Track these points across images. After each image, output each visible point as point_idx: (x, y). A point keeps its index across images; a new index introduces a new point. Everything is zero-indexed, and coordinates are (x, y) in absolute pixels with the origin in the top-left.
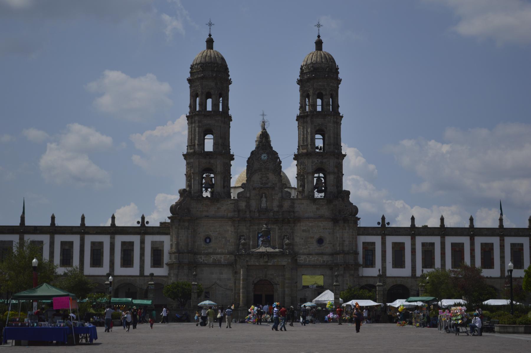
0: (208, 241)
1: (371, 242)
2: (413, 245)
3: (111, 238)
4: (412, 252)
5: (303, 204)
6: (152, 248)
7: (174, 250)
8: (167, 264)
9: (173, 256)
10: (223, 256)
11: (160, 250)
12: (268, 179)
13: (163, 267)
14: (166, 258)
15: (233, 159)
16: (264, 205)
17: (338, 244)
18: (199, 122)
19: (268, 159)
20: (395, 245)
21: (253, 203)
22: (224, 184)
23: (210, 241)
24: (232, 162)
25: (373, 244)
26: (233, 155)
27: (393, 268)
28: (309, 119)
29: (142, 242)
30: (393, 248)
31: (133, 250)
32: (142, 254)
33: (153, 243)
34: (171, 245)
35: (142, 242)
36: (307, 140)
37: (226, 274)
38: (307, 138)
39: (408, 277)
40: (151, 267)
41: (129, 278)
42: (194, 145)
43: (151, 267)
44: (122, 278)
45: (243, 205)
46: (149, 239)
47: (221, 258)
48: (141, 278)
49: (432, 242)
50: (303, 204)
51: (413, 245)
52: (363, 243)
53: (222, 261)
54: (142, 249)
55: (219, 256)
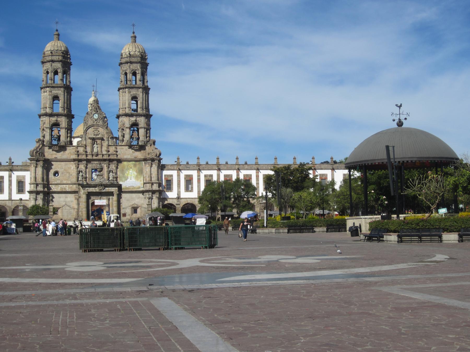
0: (57, 175)
2: (199, 176)
4: (198, 181)
6: (17, 180)
7: (33, 181)
9: (32, 185)
14: (28, 187)
15: (73, 118)
16: (95, 150)
18: (49, 92)
20: (187, 176)
21: (89, 149)
23: (58, 175)
24: (73, 120)
25: (171, 176)
26: (74, 115)
28: (127, 89)
29: (10, 176)
30: (185, 178)
32: (10, 184)
33: (17, 176)
34: (31, 178)
35: (10, 176)
36: (125, 105)
37: (71, 198)
39: (195, 198)
42: (46, 108)
45: (81, 150)
46: (15, 174)
49: (211, 174)
51: (199, 176)
53: (67, 189)
54: (10, 181)
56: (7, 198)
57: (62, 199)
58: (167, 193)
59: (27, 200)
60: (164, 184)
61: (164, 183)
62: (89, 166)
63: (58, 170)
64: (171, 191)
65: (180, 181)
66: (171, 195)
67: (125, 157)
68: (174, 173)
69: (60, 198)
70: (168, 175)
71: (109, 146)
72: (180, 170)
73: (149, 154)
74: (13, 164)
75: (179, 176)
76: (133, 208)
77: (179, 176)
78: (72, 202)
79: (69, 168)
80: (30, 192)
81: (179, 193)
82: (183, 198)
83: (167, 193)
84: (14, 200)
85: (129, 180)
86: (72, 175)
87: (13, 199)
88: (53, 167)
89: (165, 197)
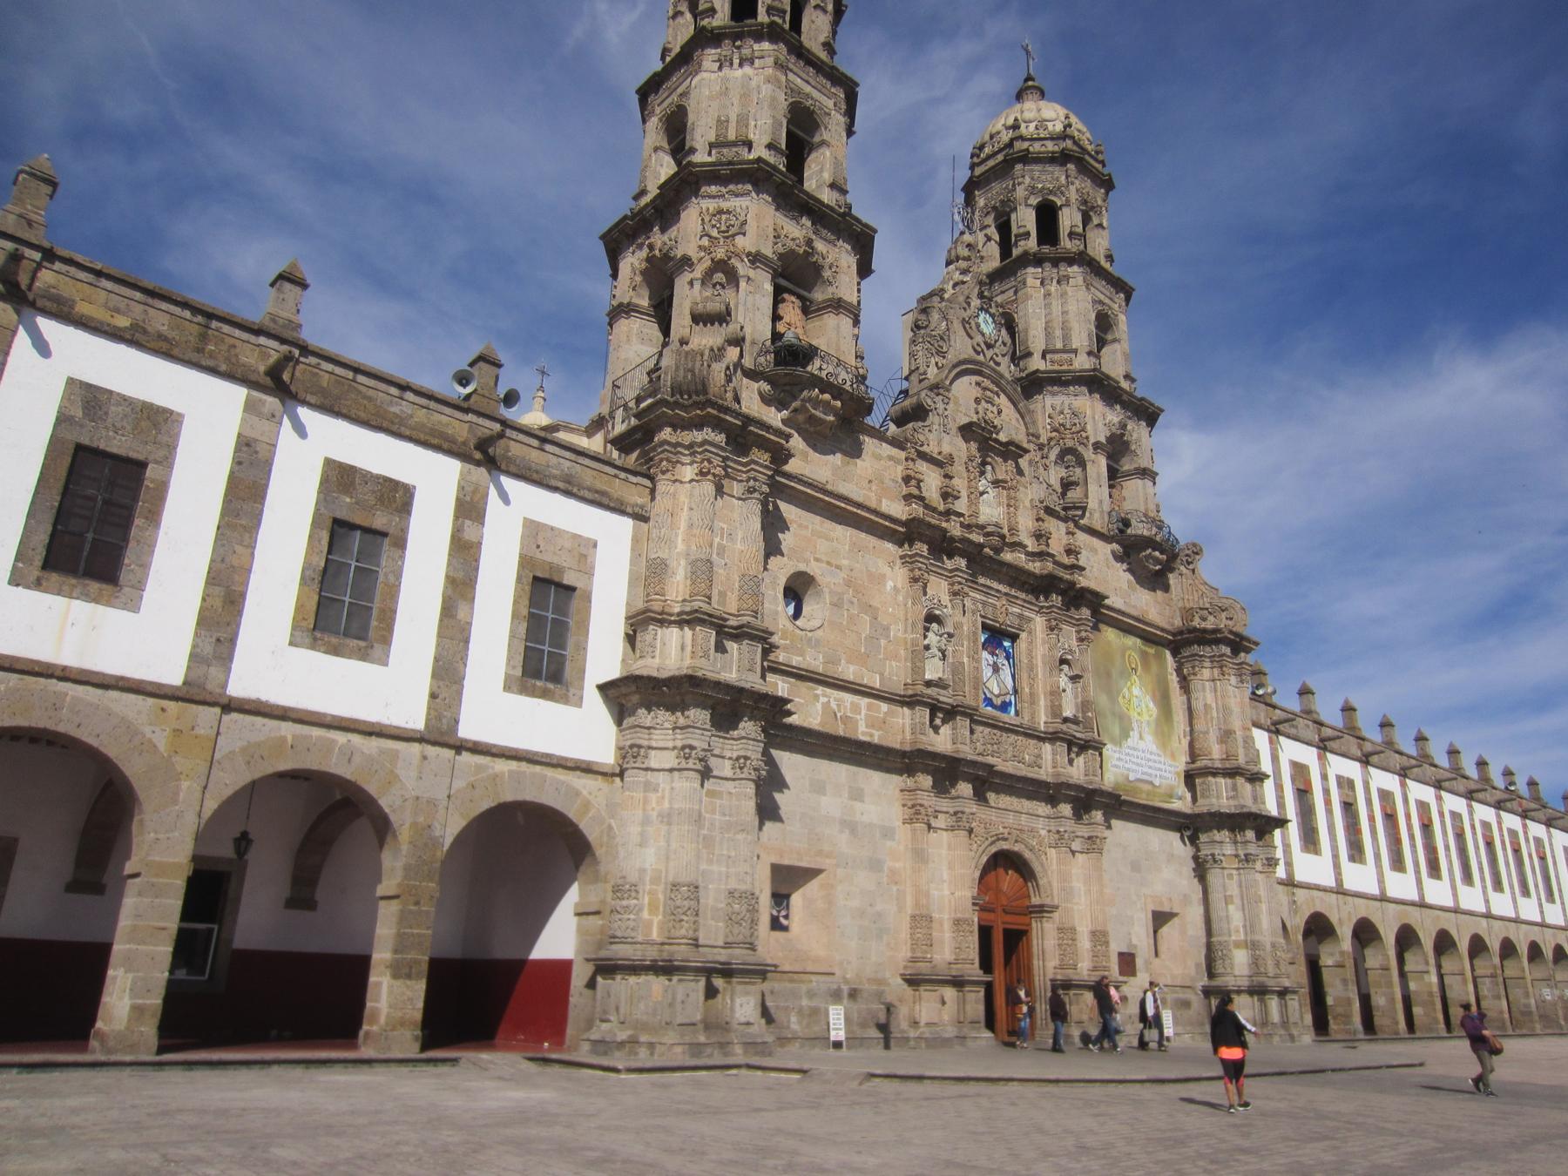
3: (250, 407)
6: (525, 562)
8: (603, 688)
11: (573, 589)
13: (579, 704)
17: (1213, 736)
31: (401, 543)
33: (534, 531)
35: (469, 509)
38: (1066, 329)
40: (507, 688)
41: (341, 738)
43: (507, 688)
44: (288, 729)
47: (856, 708)
48: (432, 751)
53: (862, 727)
54: (465, 553)
55: (848, 698)
56: (414, 717)
57: (831, 805)
59: (586, 768)
63: (813, 569)
69: (819, 788)
73: (1188, 613)
74: (509, 414)
78: (888, 833)
79: (871, 575)
80: (625, 696)
84: (477, 749)
86: (887, 629)
87: (468, 730)
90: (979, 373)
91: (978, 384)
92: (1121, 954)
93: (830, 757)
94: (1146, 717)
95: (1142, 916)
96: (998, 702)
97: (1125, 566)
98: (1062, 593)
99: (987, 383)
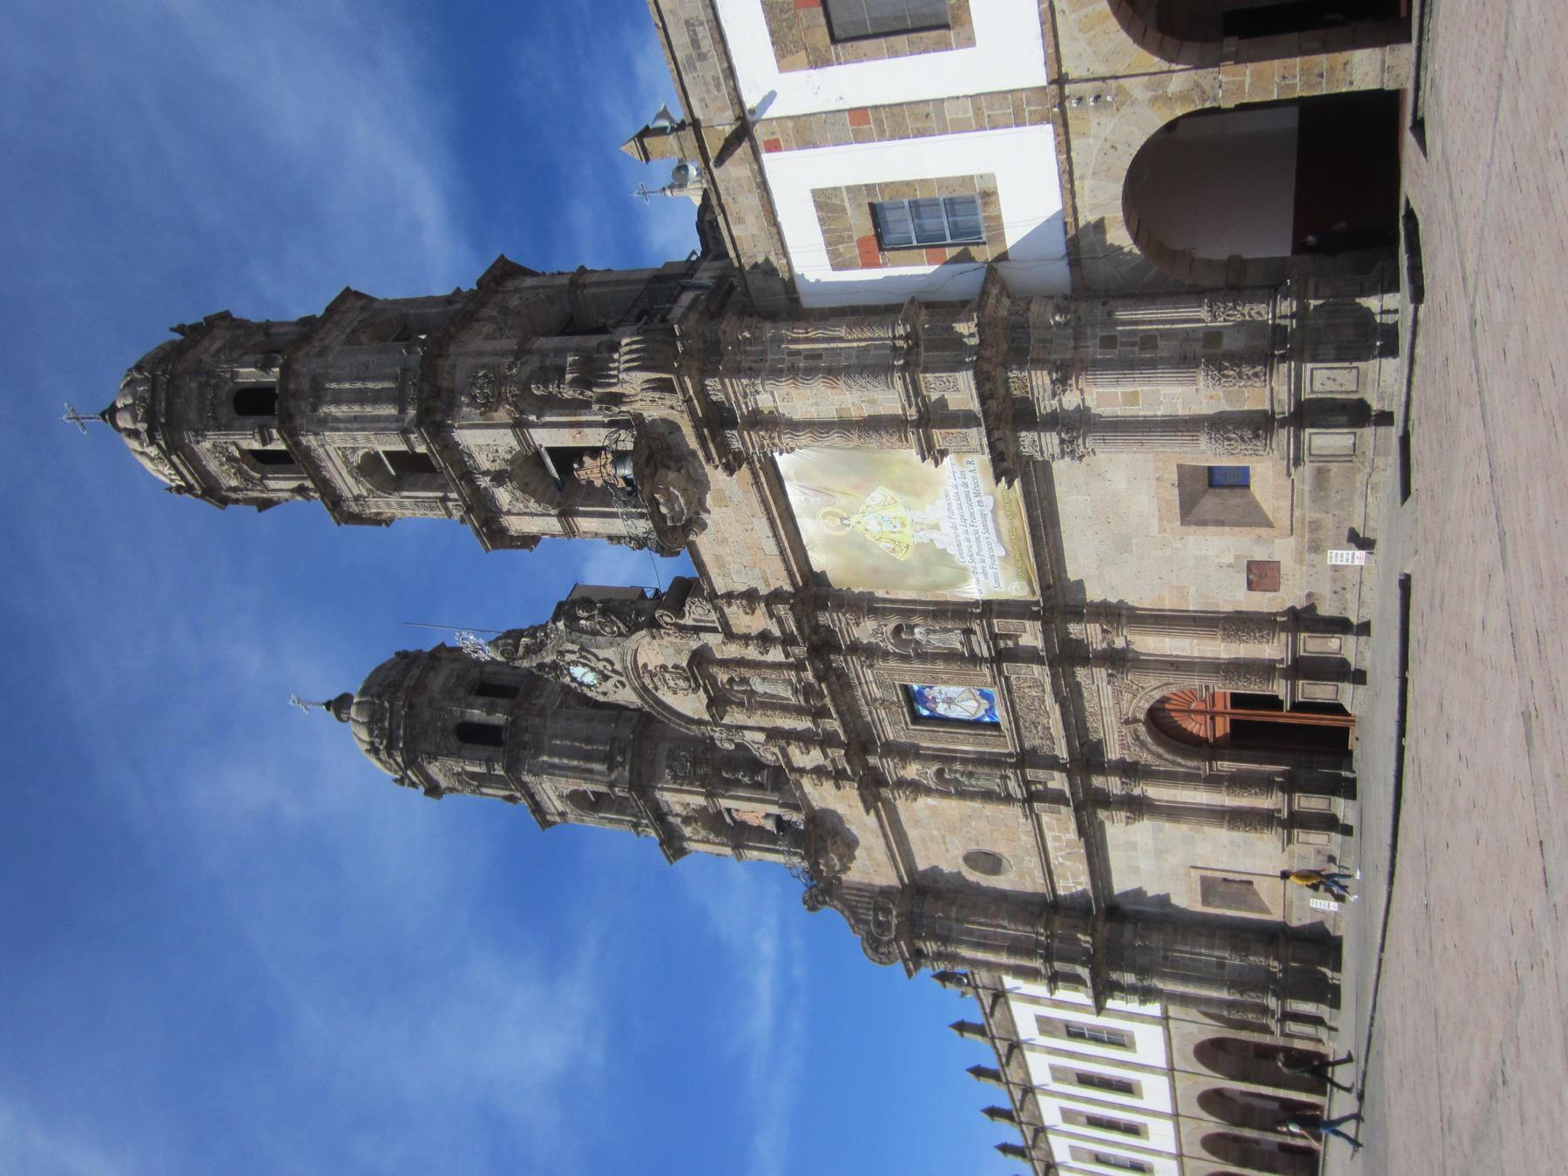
1: (822, 221)
5: (718, 557)
10: (1048, 835)
12: (664, 667)
16: (785, 692)
19: (584, 665)
22: (747, 786)
25: (826, 203)
27: (970, 41)
30: (819, 61)
50: (718, 557)
52: (837, 267)
55: (1050, 844)
57: (1146, 864)
58: (1012, 238)
60: (928, 269)
61: (916, 269)
62: (893, 727)
64: (989, 196)
65: (859, 115)
66: (1028, 190)
67: (770, 547)
68: (795, 177)
69: (1135, 870)
70: (834, 240)
71: (730, 636)
72: (743, 131)
75: (808, 131)
76: (1189, 511)
77: (808, 131)
81: (993, 110)
82: (1054, 57)
83: (1012, 238)
85: (944, 540)
88: (946, 868)
89: (1060, 248)
90: (644, 687)
91: (656, 689)
92: (1251, 586)
93: (1106, 860)
94: (899, 511)
95: (1191, 539)
96: (984, 701)
97: (704, 516)
98: (829, 667)
99: (647, 681)
